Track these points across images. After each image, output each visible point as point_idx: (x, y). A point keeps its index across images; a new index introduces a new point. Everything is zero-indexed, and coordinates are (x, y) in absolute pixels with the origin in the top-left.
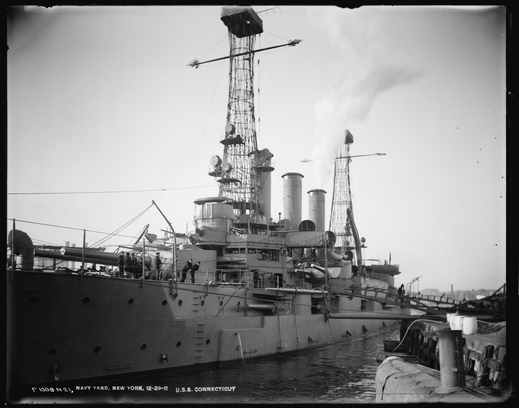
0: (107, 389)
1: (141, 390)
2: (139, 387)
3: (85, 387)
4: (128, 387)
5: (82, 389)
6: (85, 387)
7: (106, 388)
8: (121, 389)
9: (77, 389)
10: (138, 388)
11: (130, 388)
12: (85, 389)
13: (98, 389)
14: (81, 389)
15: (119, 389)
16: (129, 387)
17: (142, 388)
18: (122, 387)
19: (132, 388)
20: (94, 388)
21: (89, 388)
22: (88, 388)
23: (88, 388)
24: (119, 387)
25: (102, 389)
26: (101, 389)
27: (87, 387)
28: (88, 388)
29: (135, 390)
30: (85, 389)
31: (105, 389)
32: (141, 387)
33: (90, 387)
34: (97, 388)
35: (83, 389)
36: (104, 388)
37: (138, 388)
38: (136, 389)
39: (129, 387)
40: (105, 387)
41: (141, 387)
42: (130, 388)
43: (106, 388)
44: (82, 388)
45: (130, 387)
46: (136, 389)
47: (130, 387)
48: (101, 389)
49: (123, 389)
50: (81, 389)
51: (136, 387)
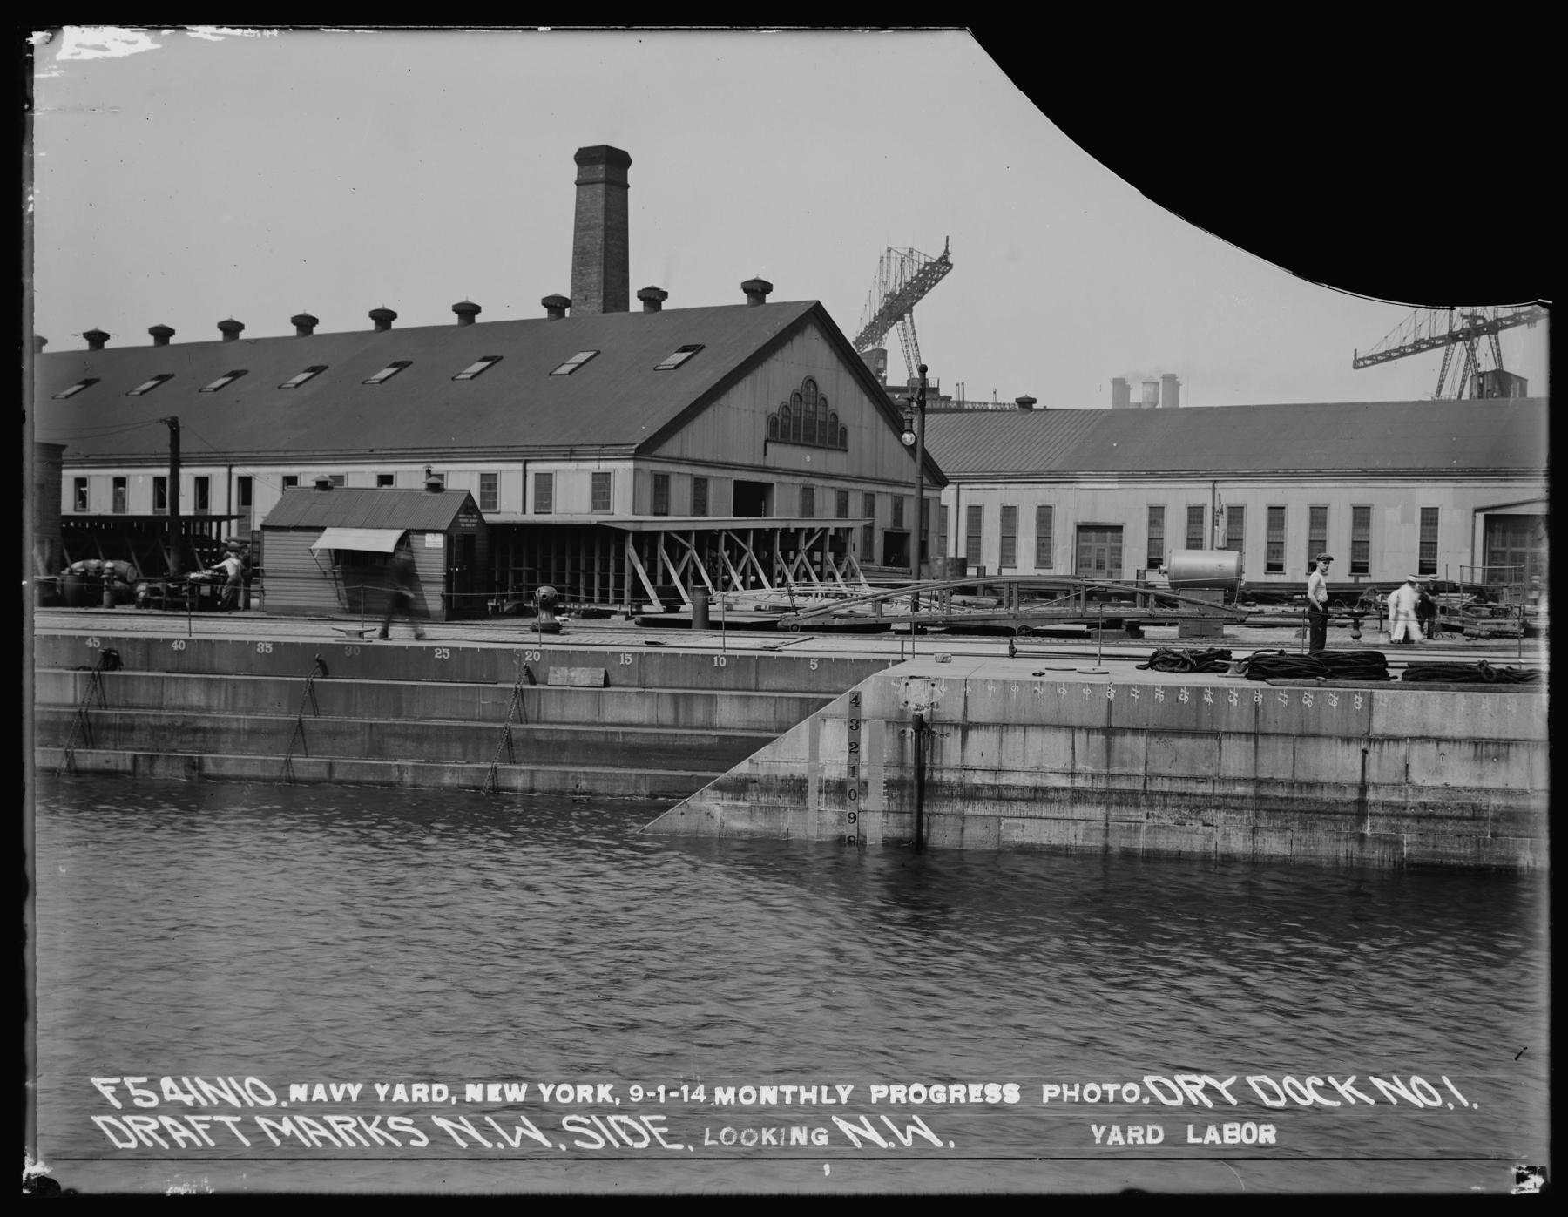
0: (444, 1097)
1: (609, 1100)
2: (600, 1087)
3: (333, 1087)
4: (541, 1086)
5: (320, 1101)
6: (333, 1087)
7: (440, 1093)
8: (510, 1098)
9: (293, 1099)
10: (594, 1095)
11: (555, 1090)
12: (338, 1097)
13: (400, 1100)
14: (314, 1099)
15: (499, 1099)
16: (547, 1087)
17: (613, 1093)
18: (515, 1086)
19: (565, 1094)
20: (378, 1096)
21: (355, 1091)
22: (346, 1091)
23: (347, 1097)
24: (498, 1086)
25: (420, 1099)
26: (415, 1099)
27: (343, 1087)
28: (346, 1091)
29: (580, 1100)
30: (338, 1097)
31: (435, 1098)
32: (609, 1087)
33: (359, 1086)
34: (389, 1096)
35: (326, 1100)
36: (430, 1094)
37: (594, 1095)
38: (584, 1098)
39: (547, 1087)
40: (436, 1087)
41: (609, 1087)
42: (555, 1090)
43: (440, 1093)
44: (319, 1093)
45: (552, 1087)
46: (584, 1098)
47: (552, 1087)
48: (415, 1099)
49: (521, 1097)
50: (314, 1099)
51: (580, 1088)
